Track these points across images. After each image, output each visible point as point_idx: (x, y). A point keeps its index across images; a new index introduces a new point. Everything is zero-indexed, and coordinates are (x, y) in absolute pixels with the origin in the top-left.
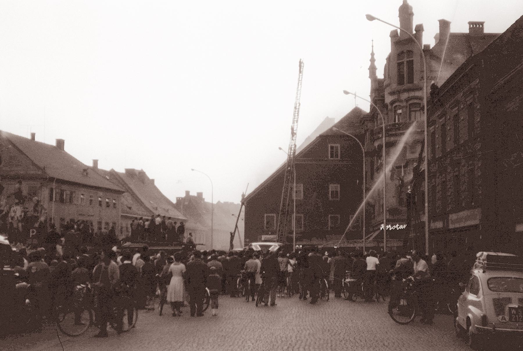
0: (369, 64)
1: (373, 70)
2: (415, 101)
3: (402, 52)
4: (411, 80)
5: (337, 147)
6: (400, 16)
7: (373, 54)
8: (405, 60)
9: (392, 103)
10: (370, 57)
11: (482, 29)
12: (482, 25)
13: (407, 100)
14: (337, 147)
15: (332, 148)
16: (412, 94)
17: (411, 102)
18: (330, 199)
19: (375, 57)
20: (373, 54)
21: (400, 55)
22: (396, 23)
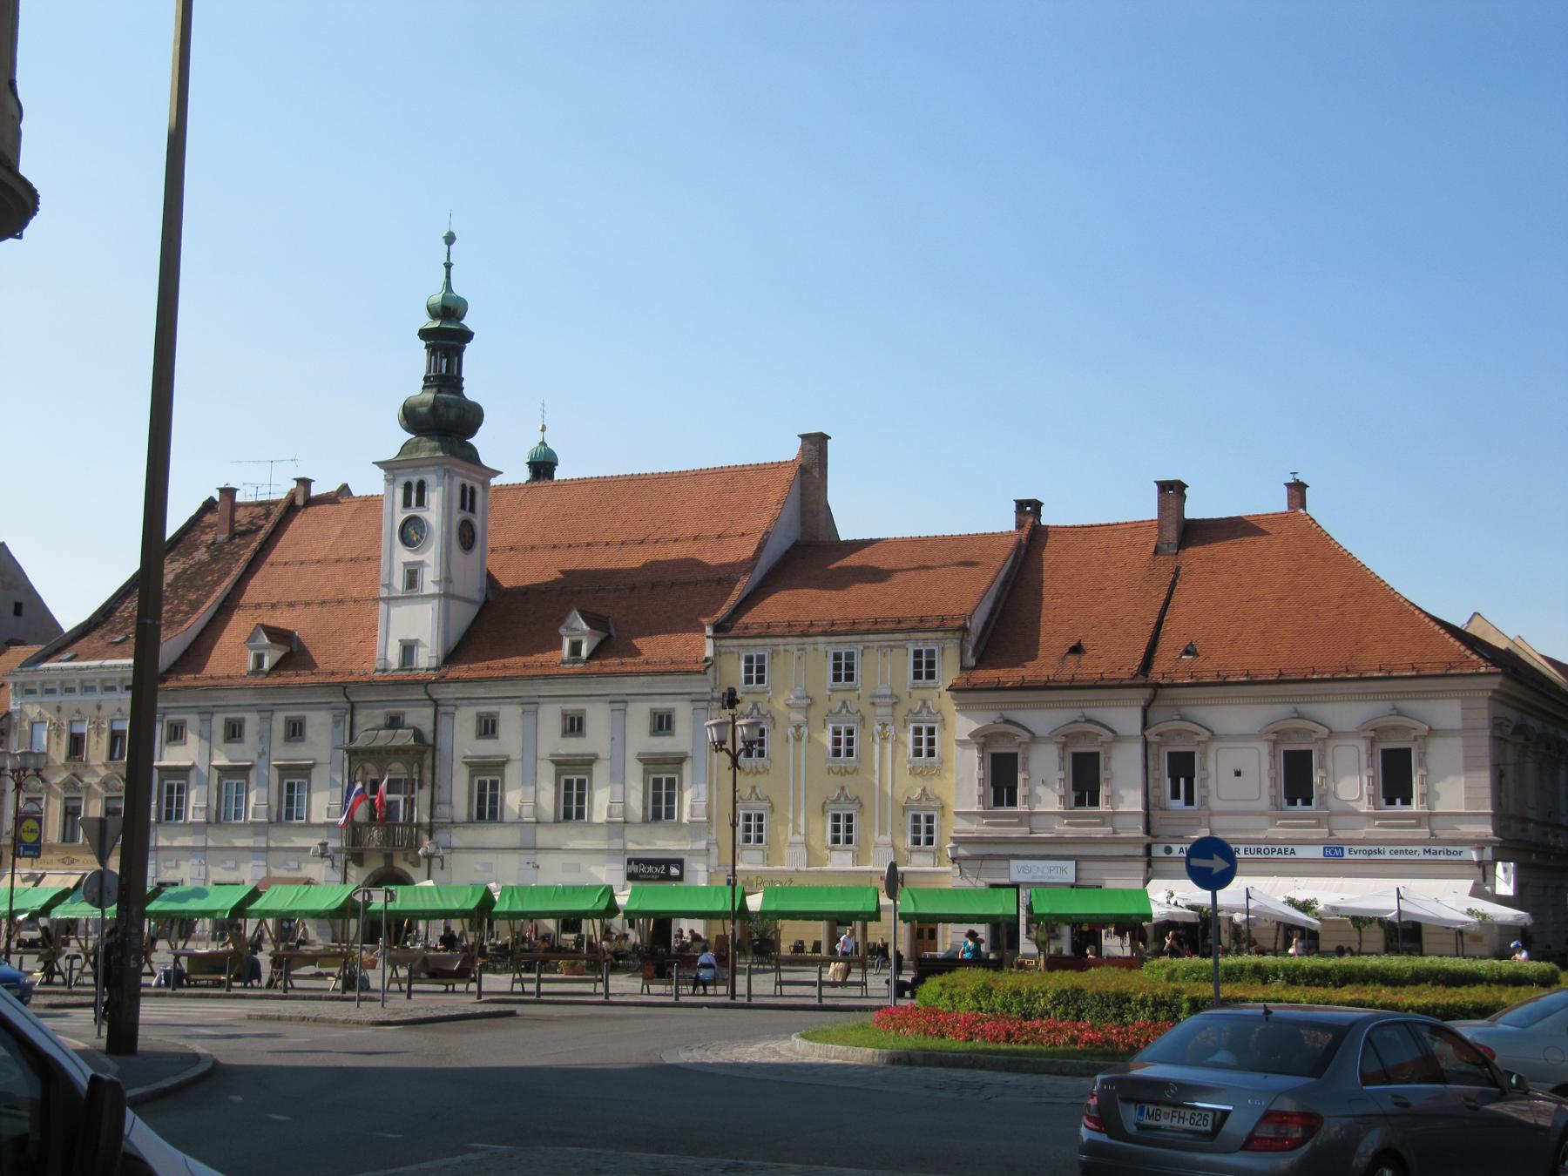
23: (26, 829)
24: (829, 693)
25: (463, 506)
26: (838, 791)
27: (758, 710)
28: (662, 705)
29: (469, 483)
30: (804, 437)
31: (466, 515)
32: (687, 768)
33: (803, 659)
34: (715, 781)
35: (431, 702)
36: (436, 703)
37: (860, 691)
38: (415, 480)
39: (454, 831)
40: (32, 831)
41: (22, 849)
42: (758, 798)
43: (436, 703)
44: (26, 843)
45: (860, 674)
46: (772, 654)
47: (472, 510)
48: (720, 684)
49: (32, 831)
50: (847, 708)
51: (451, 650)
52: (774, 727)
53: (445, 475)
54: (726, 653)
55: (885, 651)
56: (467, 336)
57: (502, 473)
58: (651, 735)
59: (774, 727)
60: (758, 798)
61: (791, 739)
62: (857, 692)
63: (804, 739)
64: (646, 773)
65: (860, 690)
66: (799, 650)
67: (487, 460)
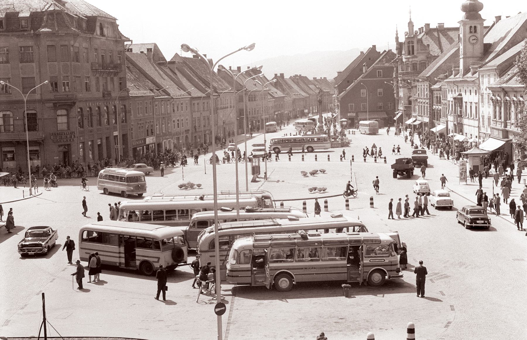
0: (395, 36)
1: (397, 38)
2: (415, 62)
3: (410, 41)
4: (413, 54)
5: (381, 72)
6: (409, 26)
7: (397, 31)
8: (411, 45)
9: (406, 62)
10: (396, 33)
11: (443, 26)
12: (443, 24)
13: (411, 62)
14: (381, 72)
15: (378, 72)
16: (414, 59)
17: (413, 62)
18: (378, 96)
19: (398, 32)
20: (397, 31)
21: (409, 43)
22: (407, 30)
29: (473, 26)
47: (475, 31)
67: (483, 17)
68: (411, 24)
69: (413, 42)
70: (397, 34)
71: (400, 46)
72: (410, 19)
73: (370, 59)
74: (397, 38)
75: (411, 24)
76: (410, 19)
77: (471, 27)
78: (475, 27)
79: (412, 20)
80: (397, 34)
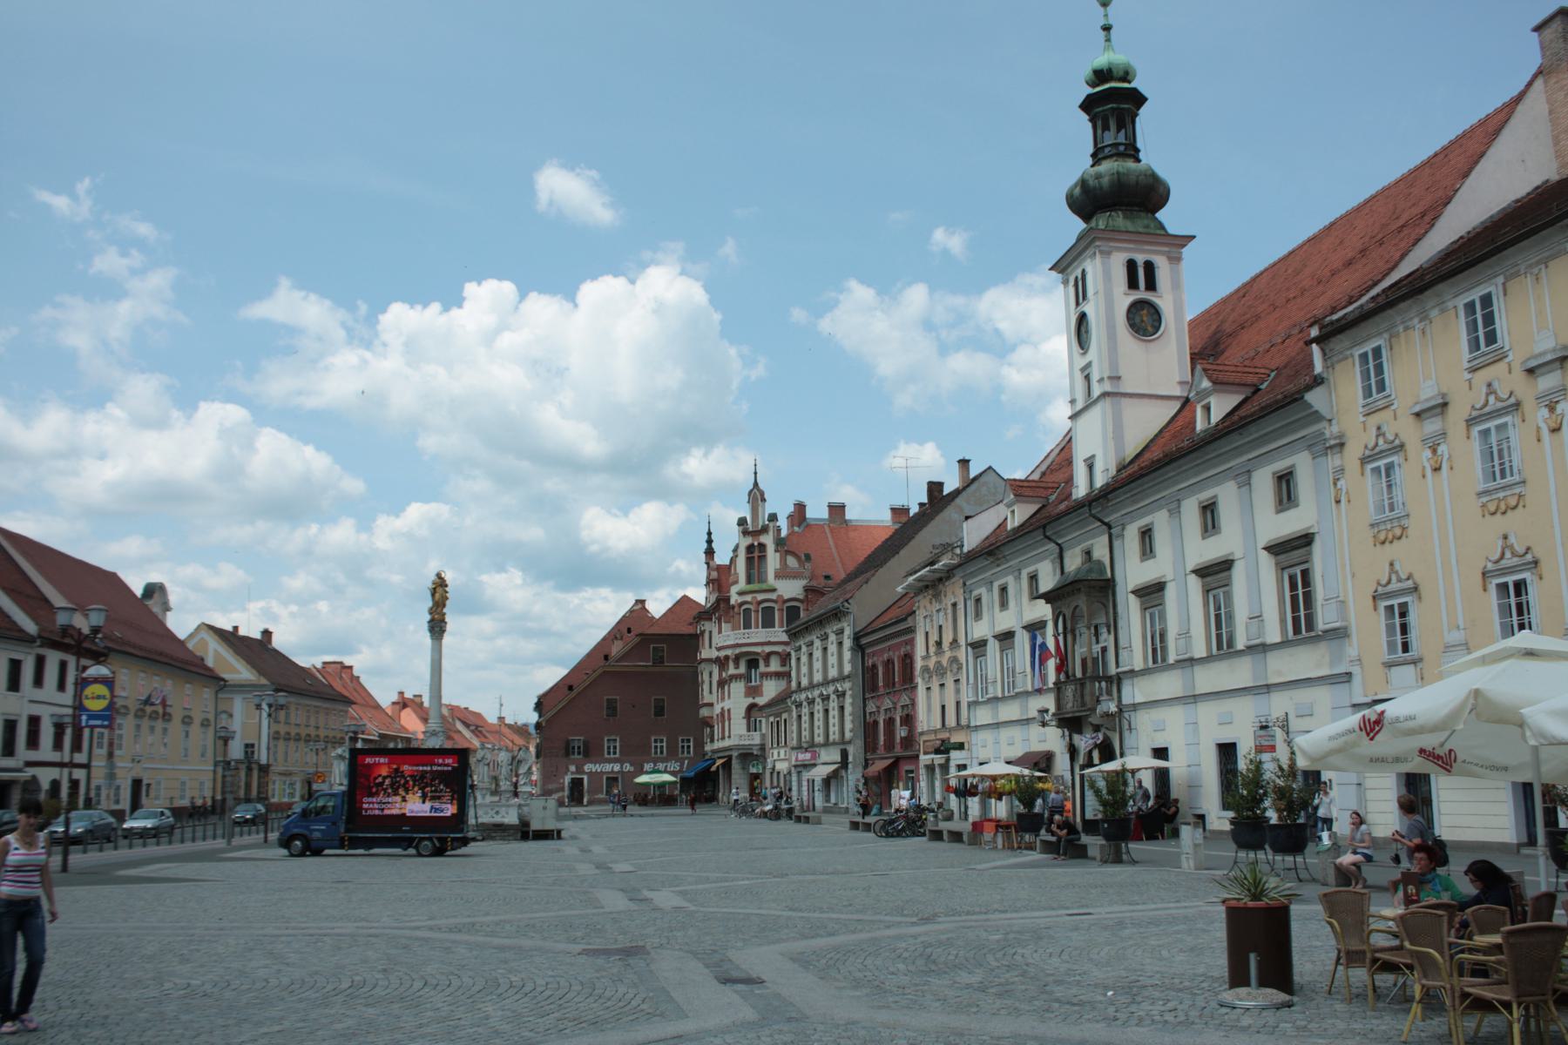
1: (710, 552)
7: (709, 534)
10: (706, 537)
19: (713, 537)
20: (709, 534)
23: (90, 696)
24: (1468, 376)
25: (1133, 284)
26: (1500, 543)
27: (1384, 435)
28: (1281, 465)
29: (1140, 259)
30: (1538, 29)
31: (1142, 294)
32: (1317, 548)
33: (1428, 331)
34: (1348, 562)
35: (1104, 527)
36: (1109, 526)
37: (1510, 358)
38: (1078, 273)
39: (1135, 680)
40: (99, 697)
41: (84, 718)
42: (1400, 580)
43: (1109, 526)
44: (87, 710)
45: (1505, 328)
46: (1390, 340)
47: (1151, 285)
48: (1338, 411)
49: (99, 697)
50: (1495, 393)
51: (1128, 460)
52: (1406, 460)
53: (1095, 253)
54: (1339, 361)
55: (1536, 270)
56: (1138, 99)
57: (1194, 237)
58: (1278, 511)
59: (1406, 460)
60: (1400, 580)
61: (1429, 472)
62: (1507, 360)
63: (1445, 466)
64: (1281, 568)
65: (1510, 353)
66: (1420, 321)
68: (756, 496)
69: (762, 547)
70: (710, 541)
71: (719, 579)
72: (756, 484)
73: (629, 631)
74: (710, 552)
75: (756, 496)
76: (756, 484)
77: (1131, 266)
78: (1150, 267)
79: (761, 486)
80: (710, 541)
